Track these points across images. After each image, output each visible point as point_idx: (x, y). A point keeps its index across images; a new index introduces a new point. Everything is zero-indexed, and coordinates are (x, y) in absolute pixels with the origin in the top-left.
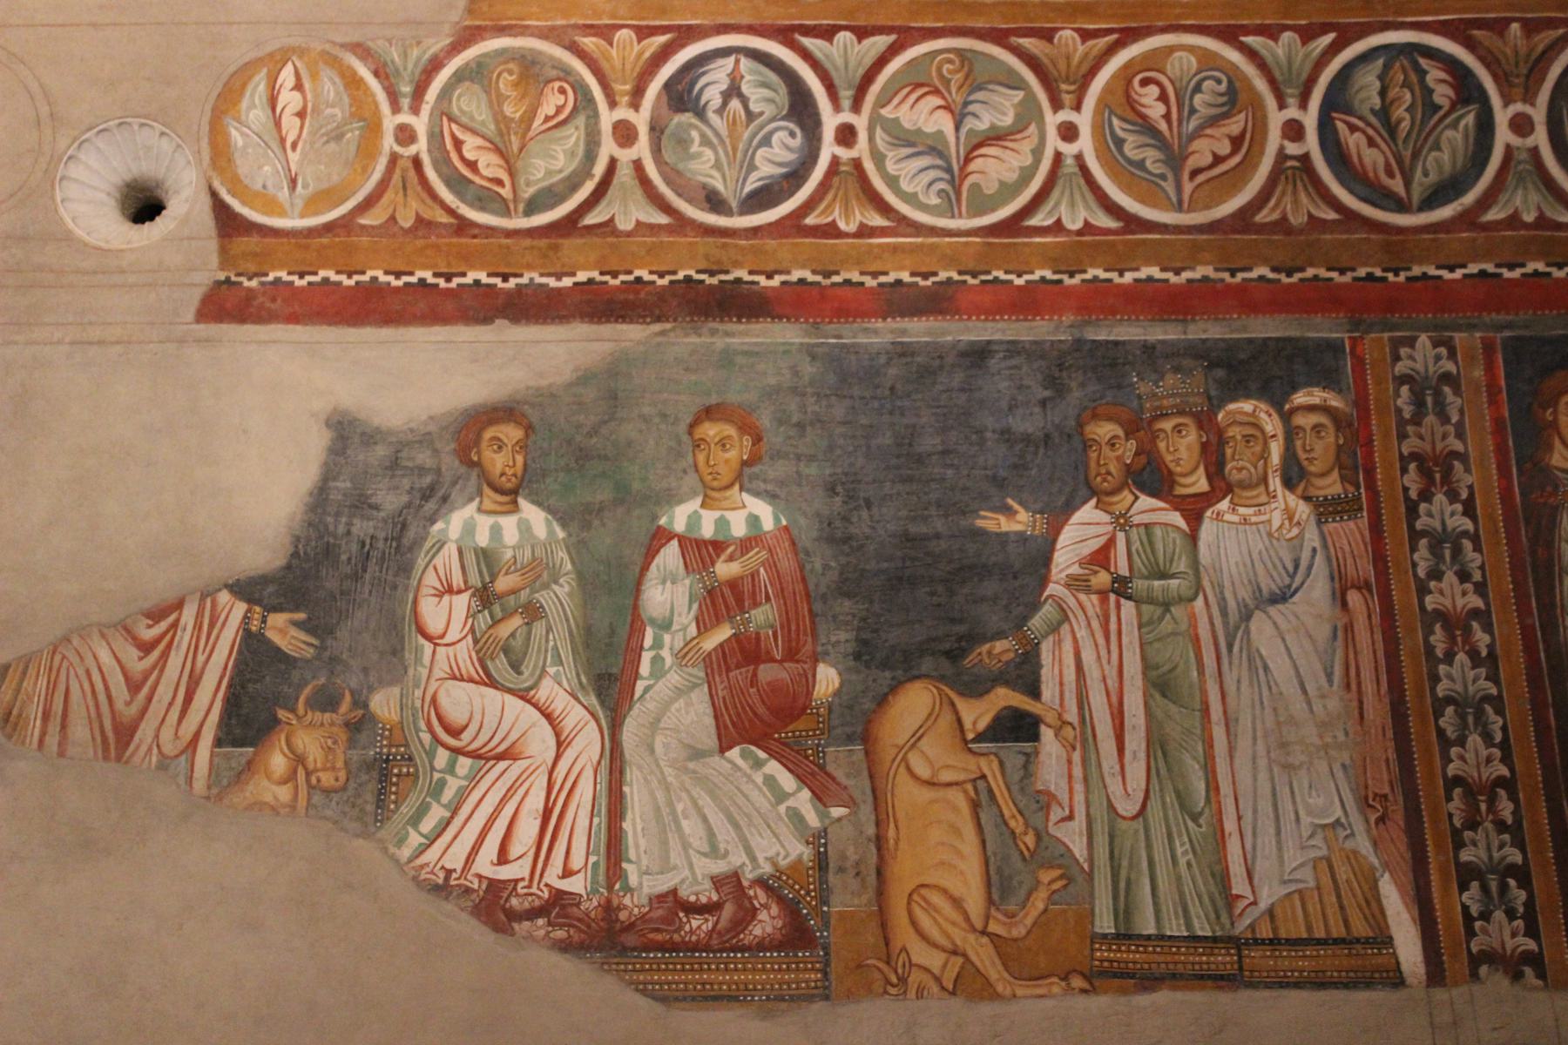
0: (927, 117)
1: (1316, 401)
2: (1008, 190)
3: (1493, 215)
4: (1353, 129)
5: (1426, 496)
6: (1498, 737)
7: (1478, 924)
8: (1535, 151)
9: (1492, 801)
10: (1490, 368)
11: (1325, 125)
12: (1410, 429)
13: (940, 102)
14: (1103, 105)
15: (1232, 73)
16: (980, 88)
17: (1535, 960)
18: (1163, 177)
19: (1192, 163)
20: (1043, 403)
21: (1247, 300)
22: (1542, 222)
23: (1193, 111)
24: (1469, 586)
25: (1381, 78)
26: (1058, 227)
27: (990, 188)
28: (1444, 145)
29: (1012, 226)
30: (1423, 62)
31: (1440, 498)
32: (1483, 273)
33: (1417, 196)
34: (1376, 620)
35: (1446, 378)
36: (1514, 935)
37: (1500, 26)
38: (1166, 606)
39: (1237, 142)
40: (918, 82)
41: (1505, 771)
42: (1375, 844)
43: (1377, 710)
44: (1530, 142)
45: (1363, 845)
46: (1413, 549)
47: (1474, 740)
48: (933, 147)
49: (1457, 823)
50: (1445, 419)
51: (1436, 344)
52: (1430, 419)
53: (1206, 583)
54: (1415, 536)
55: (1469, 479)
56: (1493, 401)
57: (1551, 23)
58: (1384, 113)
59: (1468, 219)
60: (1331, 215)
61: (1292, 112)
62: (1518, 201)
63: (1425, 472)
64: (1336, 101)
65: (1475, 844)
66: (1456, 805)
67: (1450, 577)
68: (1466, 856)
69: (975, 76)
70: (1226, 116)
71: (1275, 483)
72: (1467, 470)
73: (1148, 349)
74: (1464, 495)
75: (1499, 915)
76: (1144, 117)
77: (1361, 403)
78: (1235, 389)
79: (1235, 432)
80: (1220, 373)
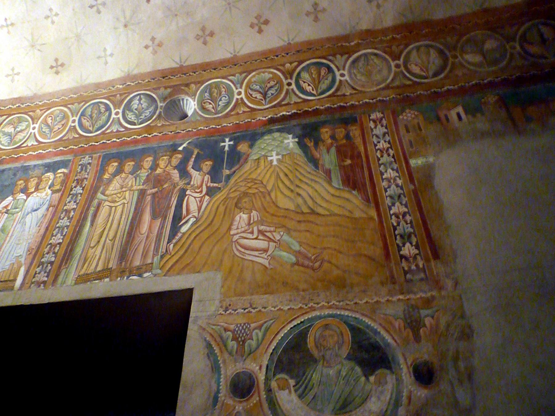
0: (10, 129)
1: (62, 171)
2: (21, 140)
3: (109, 131)
4: (85, 119)
5: (75, 187)
6: (64, 234)
7: (37, 275)
8: (119, 118)
9: (54, 248)
10: (98, 161)
11: (80, 119)
12: (78, 174)
13: (12, 126)
14: (42, 122)
15: (65, 112)
16: (21, 123)
17: (44, 283)
18: (48, 134)
19: (54, 130)
20: (11, 179)
21: (56, 154)
22: (118, 131)
23: (56, 120)
24: (75, 204)
25: (91, 109)
26: (27, 146)
27: (17, 140)
28: (102, 120)
29: (19, 147)
30: (100, 104)
31: (78, 187)
32: (103, 143)
33: (95, 129)
34: (53, 212)
35: (89, 164)
36: (44, 277)
37: (115, 96)
38: (13, 214)
39: (63, 125)
40: (9, 123)
41: (61, 241)
42: (25, 259)
43: (42, 231)
44: (118, 116)
45: (23, 260)
46: (68, 197)
47: (59, 235)
48: (9, 135)
49: (45, 253)
50: (86, 171)
51: (89, 157)
52: (83, 172)
53: (23, 209)
54: (70, 194)
55: (86, 183)
56: (97, 167)
57: (125, 93)
58: (91, 116)
59: (103, 133)
60: (78, 136)
61: (74, 118)
62: (113, 128)
63: (78, 183)
64: (83, 114)
65: (46, 257)
66: (46, 250)
67: (72, 202)
68: (43, 260)
69: (20, 120)
70: (62, 120)
71: (47, 188)
72: (86, 181)
73: (35, 166)
74: (84, 186)
75: (43, 273)
76: (47, 123)
77: (70, 171)
78: (47, 172)
79: (44, 179)
80: (46, 169)
